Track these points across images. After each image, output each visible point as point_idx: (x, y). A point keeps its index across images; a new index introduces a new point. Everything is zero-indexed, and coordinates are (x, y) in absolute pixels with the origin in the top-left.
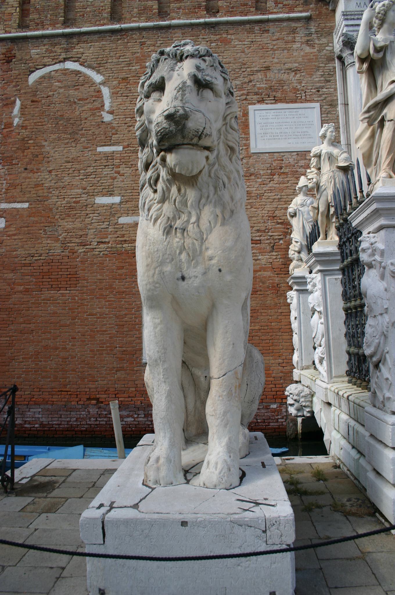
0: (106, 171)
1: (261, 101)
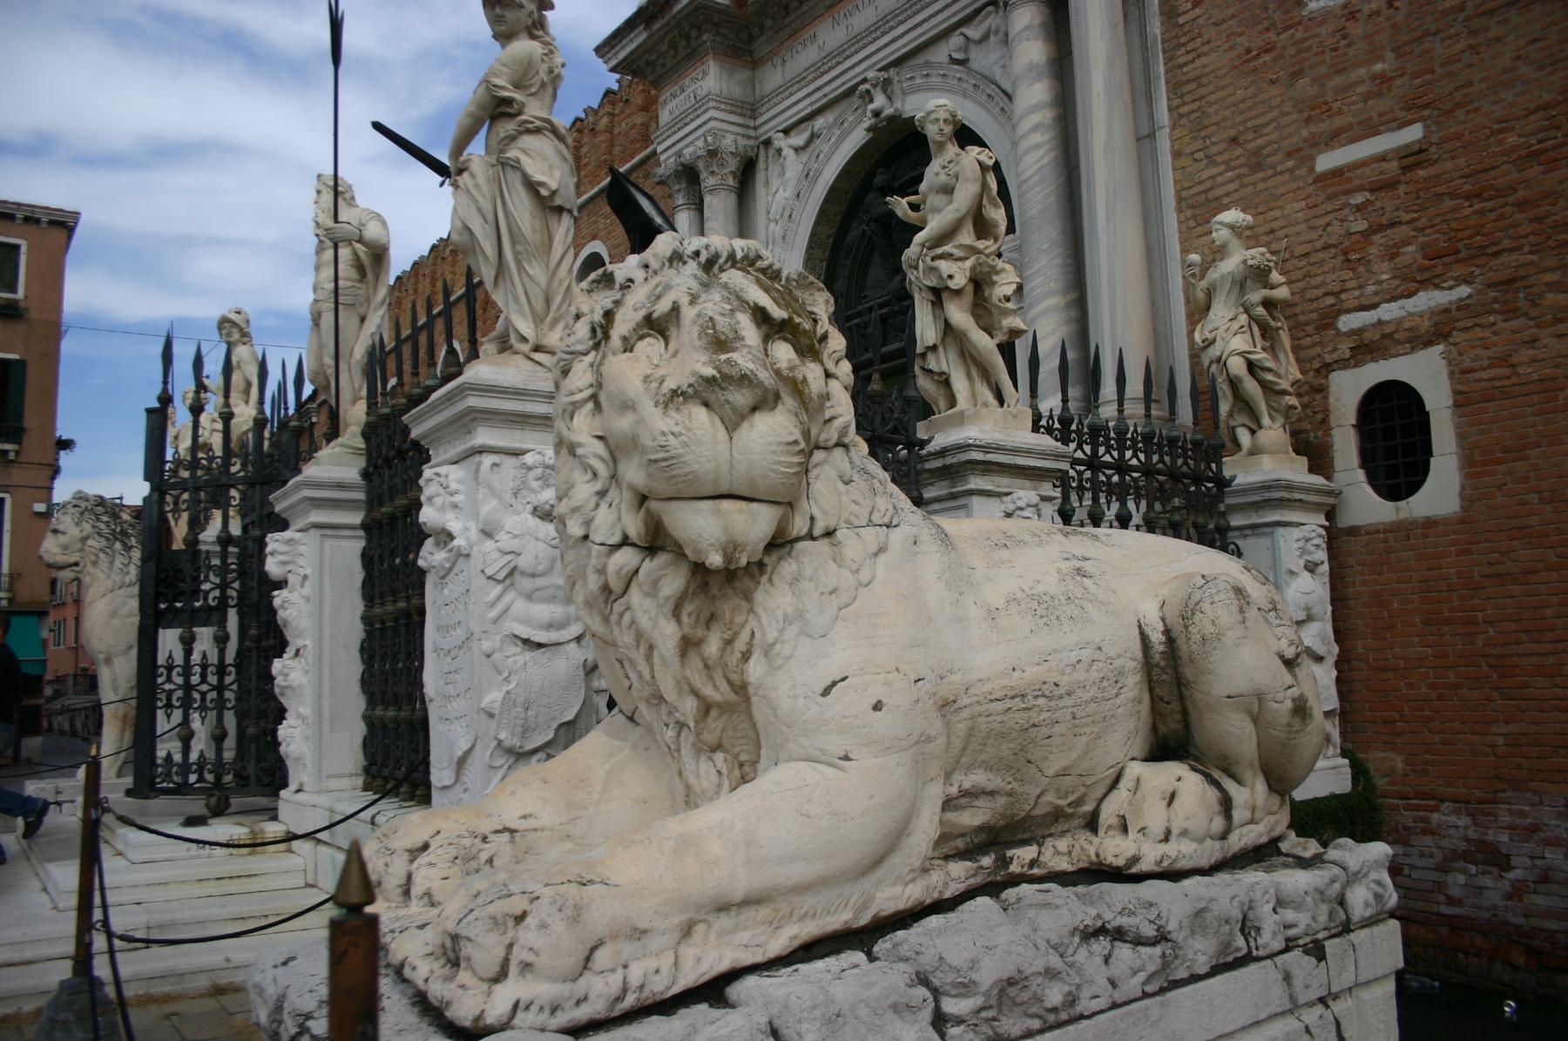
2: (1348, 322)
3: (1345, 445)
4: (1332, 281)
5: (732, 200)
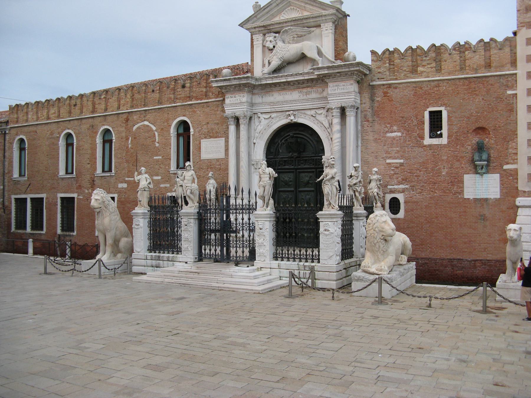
0: (157, 167)
1: (205, 138)
2: (389, 187)
3: (387, 205)
4: (388, 180)
5: (247, 125)
